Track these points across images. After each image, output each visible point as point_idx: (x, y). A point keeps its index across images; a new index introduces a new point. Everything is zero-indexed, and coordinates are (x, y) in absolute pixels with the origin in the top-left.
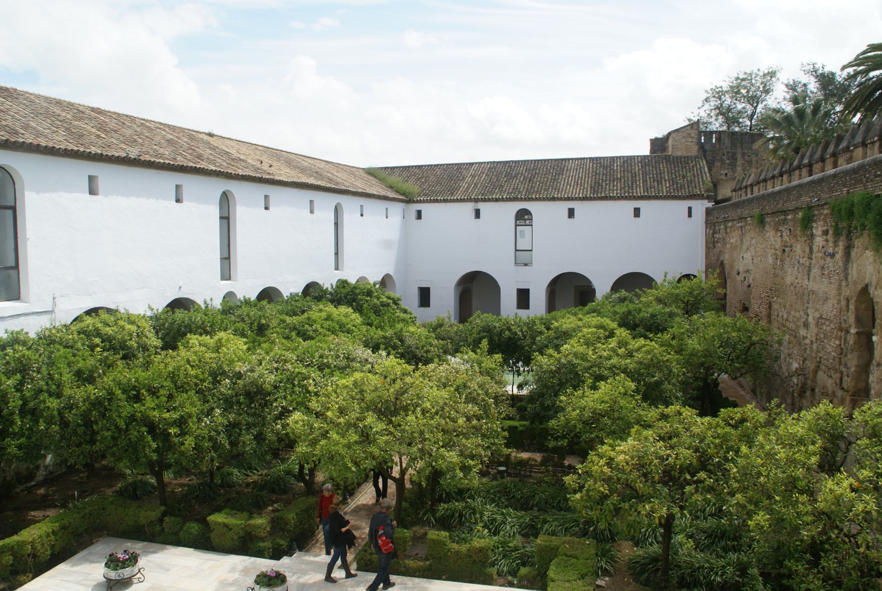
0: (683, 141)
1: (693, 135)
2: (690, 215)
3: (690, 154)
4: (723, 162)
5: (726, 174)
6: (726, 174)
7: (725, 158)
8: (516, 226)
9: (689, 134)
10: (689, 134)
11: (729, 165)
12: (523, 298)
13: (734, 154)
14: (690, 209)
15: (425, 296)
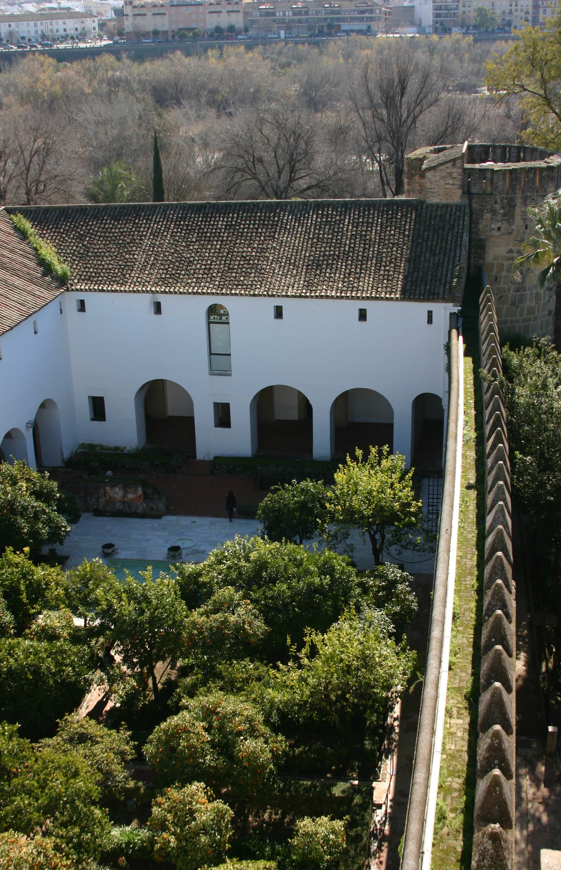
0: (442, 182)
1: (455, 175)
2: (430, 321)
3: (450, 201)
4: (494, 212)
5: (499, 229)
6: (499, 229)
7: (497, 206)
8: (209, 323)
9: (450, 174)
10: (450, 174)
11: (504, 215)
12: (223, 414)
13: (512, 200)
14: (430, 313)
15: (98, 408)
